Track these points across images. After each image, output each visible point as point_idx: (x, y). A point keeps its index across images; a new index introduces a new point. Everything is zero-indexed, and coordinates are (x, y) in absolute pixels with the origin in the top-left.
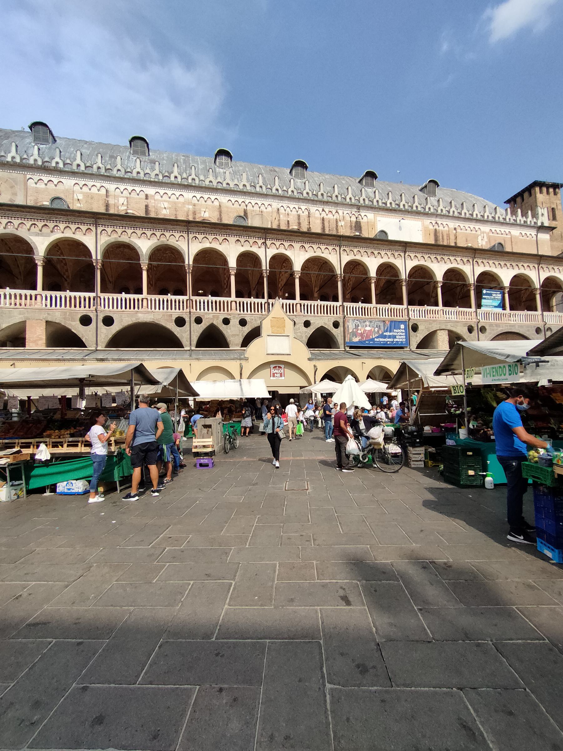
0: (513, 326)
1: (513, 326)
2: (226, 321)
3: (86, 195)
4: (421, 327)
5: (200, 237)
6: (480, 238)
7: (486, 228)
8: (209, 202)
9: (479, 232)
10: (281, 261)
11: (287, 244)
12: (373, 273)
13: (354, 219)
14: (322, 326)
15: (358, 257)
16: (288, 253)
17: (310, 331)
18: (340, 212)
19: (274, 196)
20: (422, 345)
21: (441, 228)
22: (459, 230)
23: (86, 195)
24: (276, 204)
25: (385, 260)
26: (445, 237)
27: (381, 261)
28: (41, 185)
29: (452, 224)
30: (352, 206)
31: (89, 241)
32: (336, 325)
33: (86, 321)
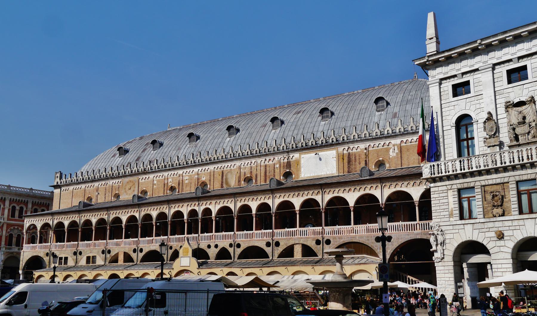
0: (353, 237)
1: (355, 237)
2: (181, 247)
3: (158, 181)
4: (281, 244)
5: (173, 206)
6: (391, 150)
7: (397, 141)
8: (206, 171)
9: (391, 146)
10: (207, 211)
11: (209, 202)
12: (254, 212)
13: (286, 160)
14: (223, 248)
15: (246, 203)
16: (210, 207)
17: (217, 250)
18: (276, 158)
19: (237, 159)
20: (281, 256)
21: (354, 150)
22: (370, 149)
23: (158, 181)
24: (238, 163)
25: (262, 201)
26: (357, 158)
27: (259, 202)
28: (143, 180)
29: (362, 146)
30: (283, 152)
31: (137, 215)
32: (231, 245)
33: (135, 251)
